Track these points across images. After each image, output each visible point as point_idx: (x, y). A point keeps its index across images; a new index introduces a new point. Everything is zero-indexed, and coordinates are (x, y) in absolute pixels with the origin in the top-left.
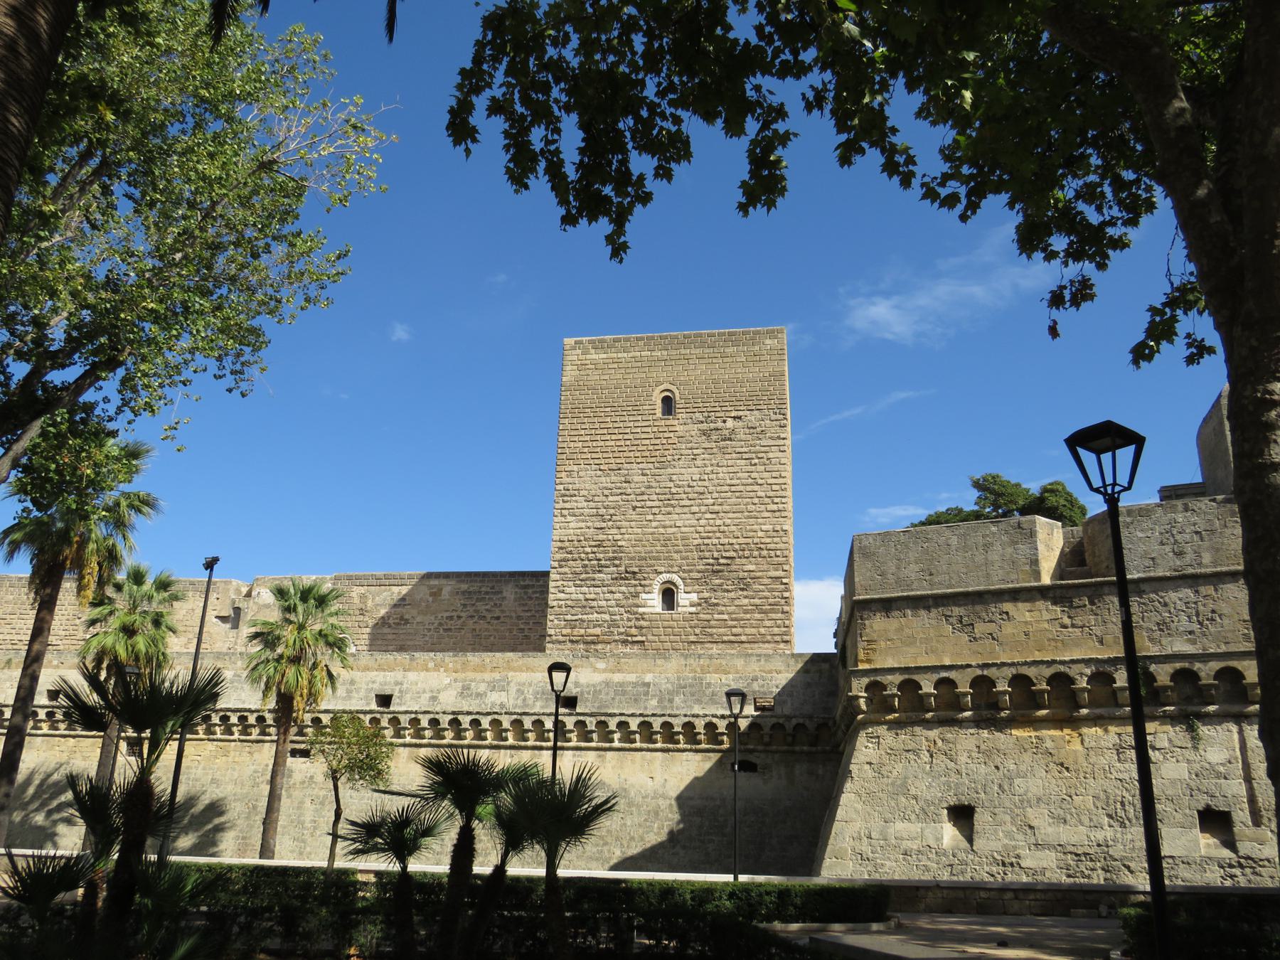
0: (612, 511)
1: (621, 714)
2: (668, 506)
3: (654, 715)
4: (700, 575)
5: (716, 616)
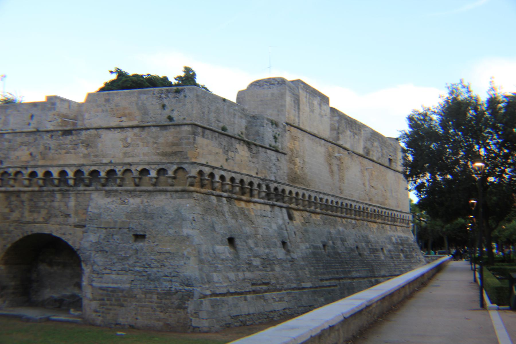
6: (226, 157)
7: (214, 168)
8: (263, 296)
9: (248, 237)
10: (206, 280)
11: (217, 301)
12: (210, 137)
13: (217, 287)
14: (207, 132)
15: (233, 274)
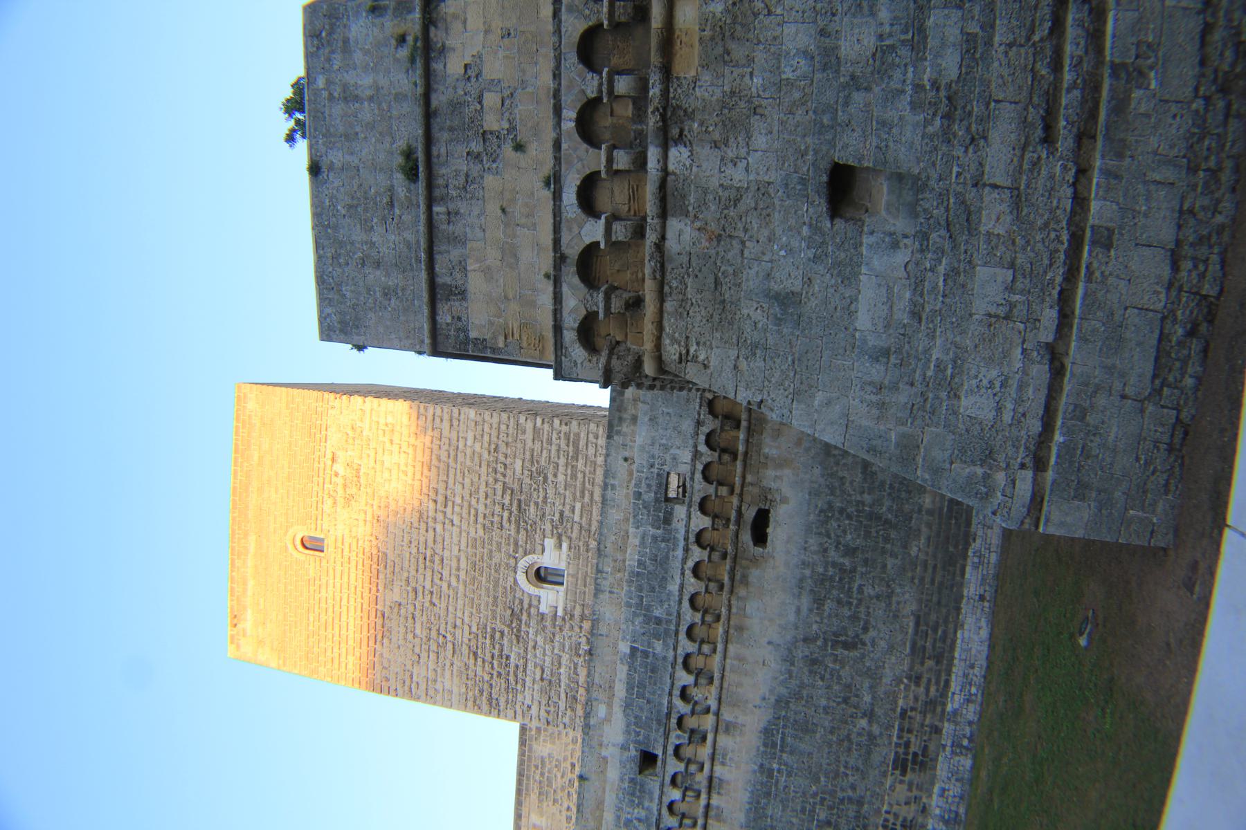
0: (434, 634)
1: (670, 694)
2: (432, 561)
3: (675, 649)
4: (522, 532)
5: (577, 518)
6: (508, 150)
7: (560, 259)
8: (1116, 69)
9: (828, 59)
10: (979, 471)
11: (1067, 448)
12: (455, 253)
13: (1017, 421)
14: (443, 279)
15: (982, 272)
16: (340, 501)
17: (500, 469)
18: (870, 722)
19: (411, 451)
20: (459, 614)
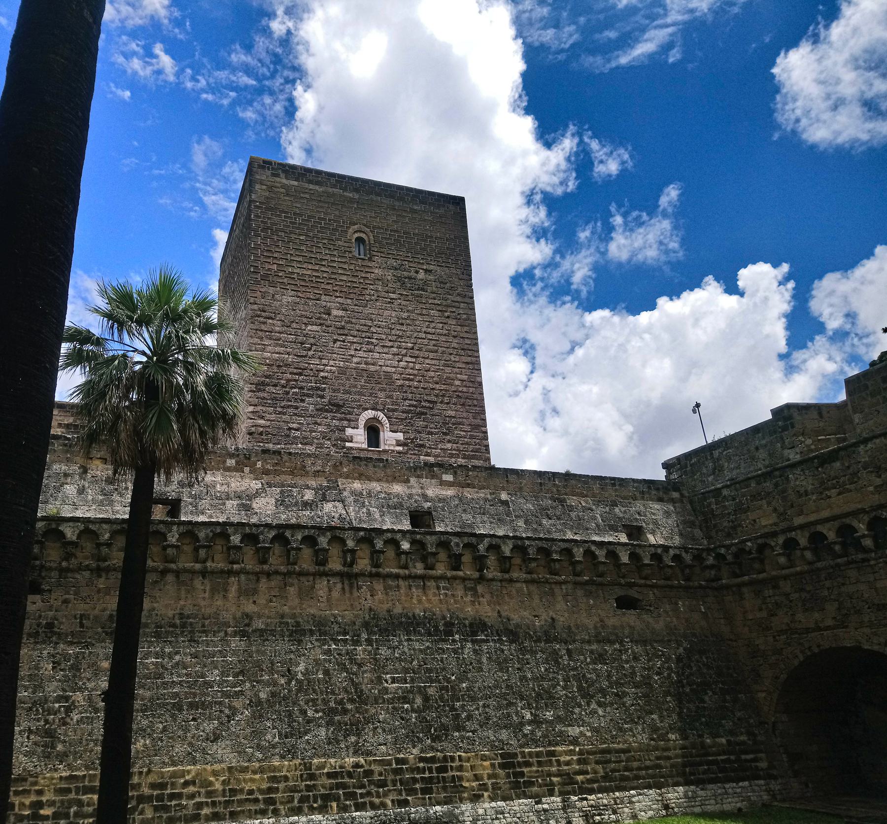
2: (368, 343)
16: (399, 273)
17: (446, 400)
18: (530, 723)
19: (445, 332)
20: (332, 363)
